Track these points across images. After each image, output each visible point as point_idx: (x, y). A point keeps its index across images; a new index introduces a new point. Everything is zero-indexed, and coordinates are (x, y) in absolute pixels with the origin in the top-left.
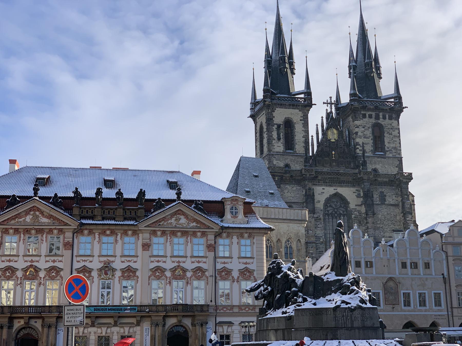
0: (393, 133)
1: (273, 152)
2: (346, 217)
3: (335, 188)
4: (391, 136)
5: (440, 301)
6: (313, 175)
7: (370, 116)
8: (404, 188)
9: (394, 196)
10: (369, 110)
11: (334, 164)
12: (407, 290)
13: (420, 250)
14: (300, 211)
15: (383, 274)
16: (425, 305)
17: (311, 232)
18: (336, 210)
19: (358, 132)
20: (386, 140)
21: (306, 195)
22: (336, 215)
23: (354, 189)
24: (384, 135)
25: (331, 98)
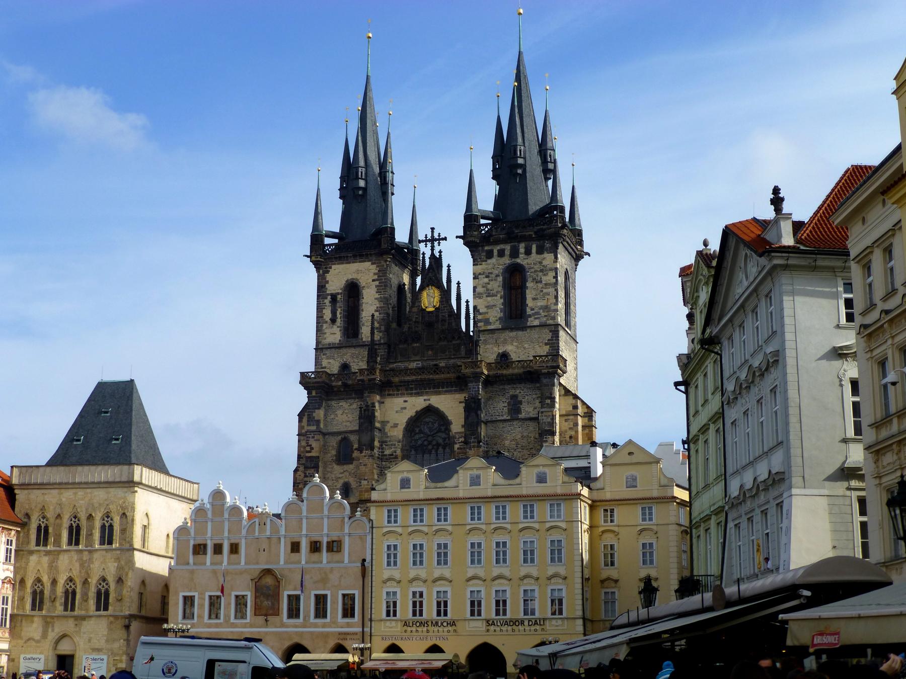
2: (447, 450)
3: (425, 397)
4: (540, 285)
5: (353, 609)
6: (375, 379)
7: (501, 254)
8: (546, 385)
10: (497, 242)
11: (430, 352)
12: (295, 589)
13: (326, 520)
14: (126, 467)
15: (257, 563)
16: (325, 616)
17: (365, 482)
20: (529, 295)
22: (430, 447)
23: (461, 396)
25: (433, 229)
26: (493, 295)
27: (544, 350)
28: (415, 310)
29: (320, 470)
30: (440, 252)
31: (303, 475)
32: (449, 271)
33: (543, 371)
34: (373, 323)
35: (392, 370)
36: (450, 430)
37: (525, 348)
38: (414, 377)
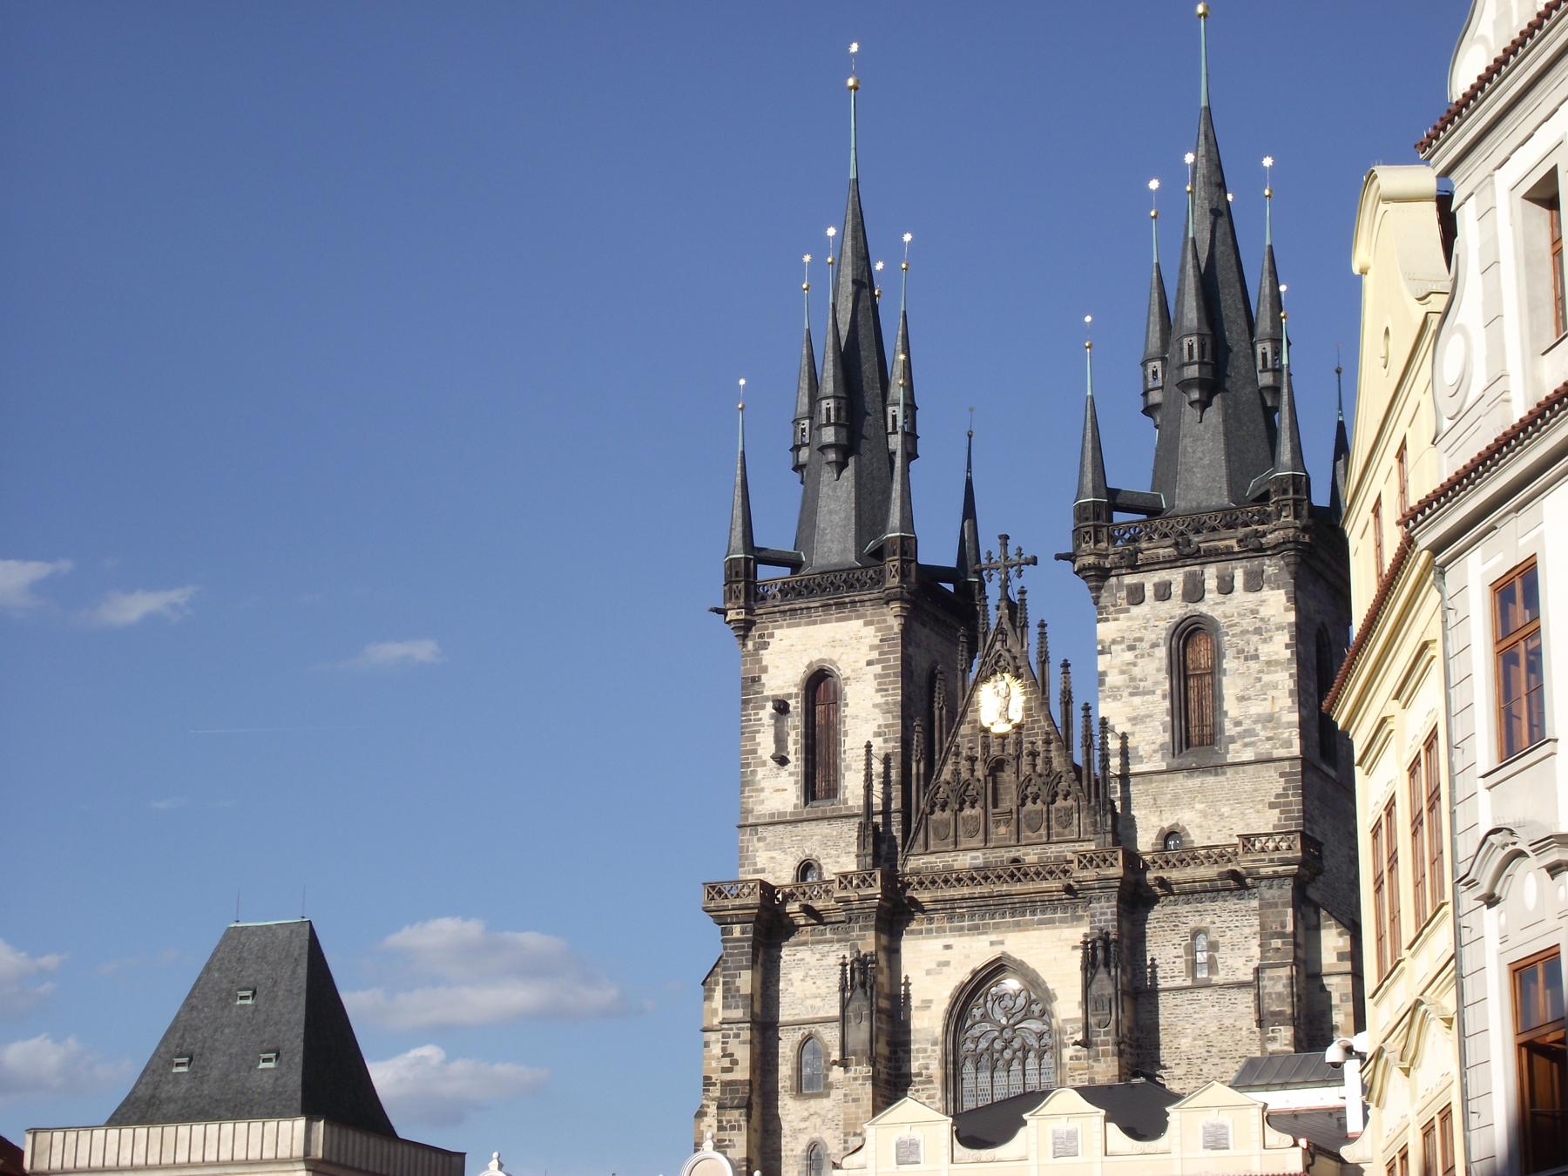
0: (1266, 651)
1: (758, 817)
3: (994, 937)
6: (873, 897)
7: (1163, 593)
9: (1254, 944)
10: (1153, 565)
11: (1002, 830)
14: (285, 1125)
18: (1007, 1034)
19: (1104, 674)
20: (1231, 688)
21: (843, 990)
22: (1008, 1054)
24: (1220, 664)
25: (1005, 538)
26: (1144, 693)
27: (1265, 820)
28: (965, 729)
29: (756, 1113)
30: (1022, 592)
31: (715, 1124)
32: (1043, 635)
33: (1263, 871)
34: (869, 765)
35: (916, 872)
36: (1052, 1015)
37: (1222, 816)
38: (966, 891)
